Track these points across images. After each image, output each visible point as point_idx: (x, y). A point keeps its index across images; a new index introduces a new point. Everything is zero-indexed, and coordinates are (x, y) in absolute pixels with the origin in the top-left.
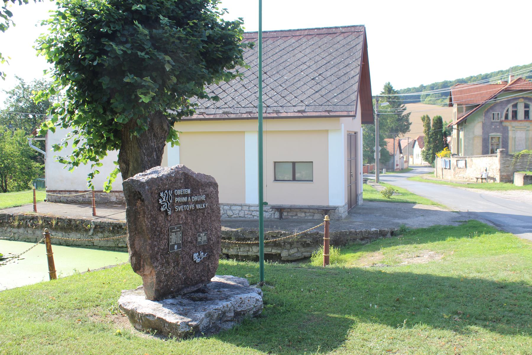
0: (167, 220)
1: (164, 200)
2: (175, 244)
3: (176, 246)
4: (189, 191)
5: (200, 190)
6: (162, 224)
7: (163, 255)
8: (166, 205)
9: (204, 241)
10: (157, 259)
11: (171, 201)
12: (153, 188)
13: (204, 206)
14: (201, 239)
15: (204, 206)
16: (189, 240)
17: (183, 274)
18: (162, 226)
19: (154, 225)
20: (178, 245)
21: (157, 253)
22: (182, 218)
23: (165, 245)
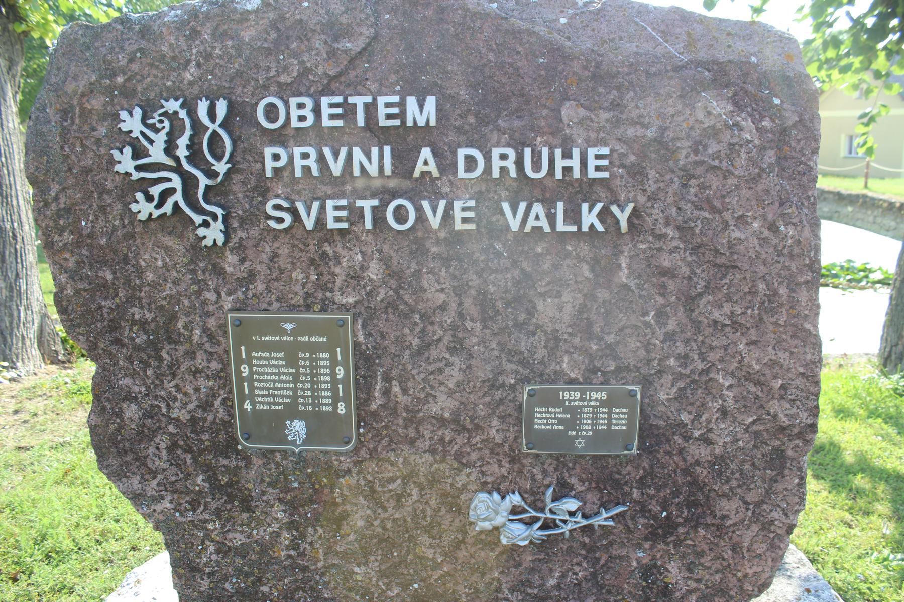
0: (218, 271)
1: (157, 154)
2: (292, 412)
3: (298, 428)
4: (423, 113)
5: (569, 112)
6: (169, 289)
7: (189, 450)
8: (176, 182)
9: (599, 437)
10: (142, 461)
11: (221, 167)
12: (70, 87)
13: (590, 218)
14: (573, 423)
15: (590, 218)
16: (443, 404)
17: (382, 575)
18: (174, 299)
19: (104, 287)
20: (322, 425)
21: (144, 435)
22: (355, 277)
23: (206, 406)
